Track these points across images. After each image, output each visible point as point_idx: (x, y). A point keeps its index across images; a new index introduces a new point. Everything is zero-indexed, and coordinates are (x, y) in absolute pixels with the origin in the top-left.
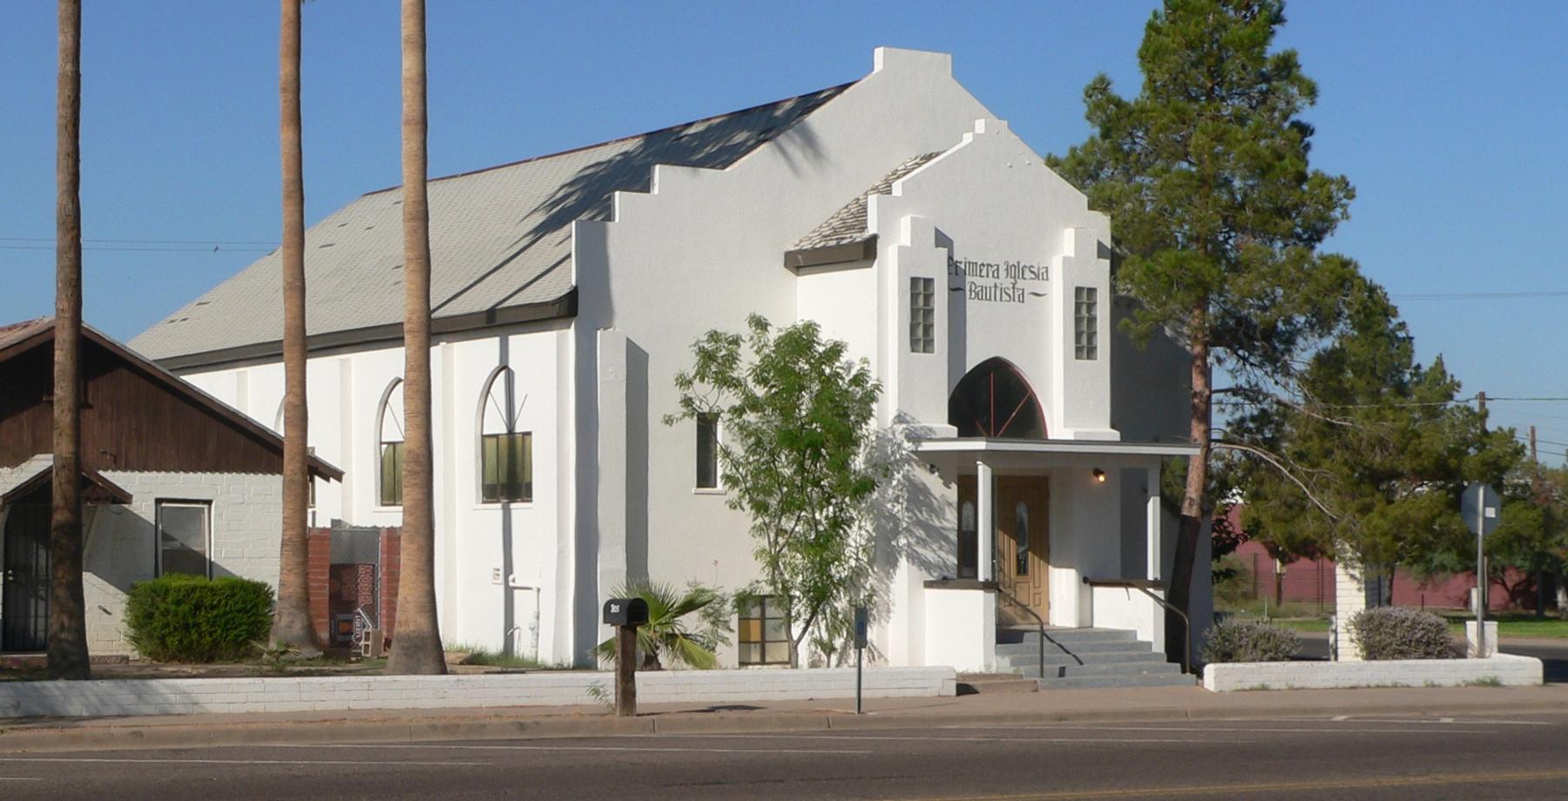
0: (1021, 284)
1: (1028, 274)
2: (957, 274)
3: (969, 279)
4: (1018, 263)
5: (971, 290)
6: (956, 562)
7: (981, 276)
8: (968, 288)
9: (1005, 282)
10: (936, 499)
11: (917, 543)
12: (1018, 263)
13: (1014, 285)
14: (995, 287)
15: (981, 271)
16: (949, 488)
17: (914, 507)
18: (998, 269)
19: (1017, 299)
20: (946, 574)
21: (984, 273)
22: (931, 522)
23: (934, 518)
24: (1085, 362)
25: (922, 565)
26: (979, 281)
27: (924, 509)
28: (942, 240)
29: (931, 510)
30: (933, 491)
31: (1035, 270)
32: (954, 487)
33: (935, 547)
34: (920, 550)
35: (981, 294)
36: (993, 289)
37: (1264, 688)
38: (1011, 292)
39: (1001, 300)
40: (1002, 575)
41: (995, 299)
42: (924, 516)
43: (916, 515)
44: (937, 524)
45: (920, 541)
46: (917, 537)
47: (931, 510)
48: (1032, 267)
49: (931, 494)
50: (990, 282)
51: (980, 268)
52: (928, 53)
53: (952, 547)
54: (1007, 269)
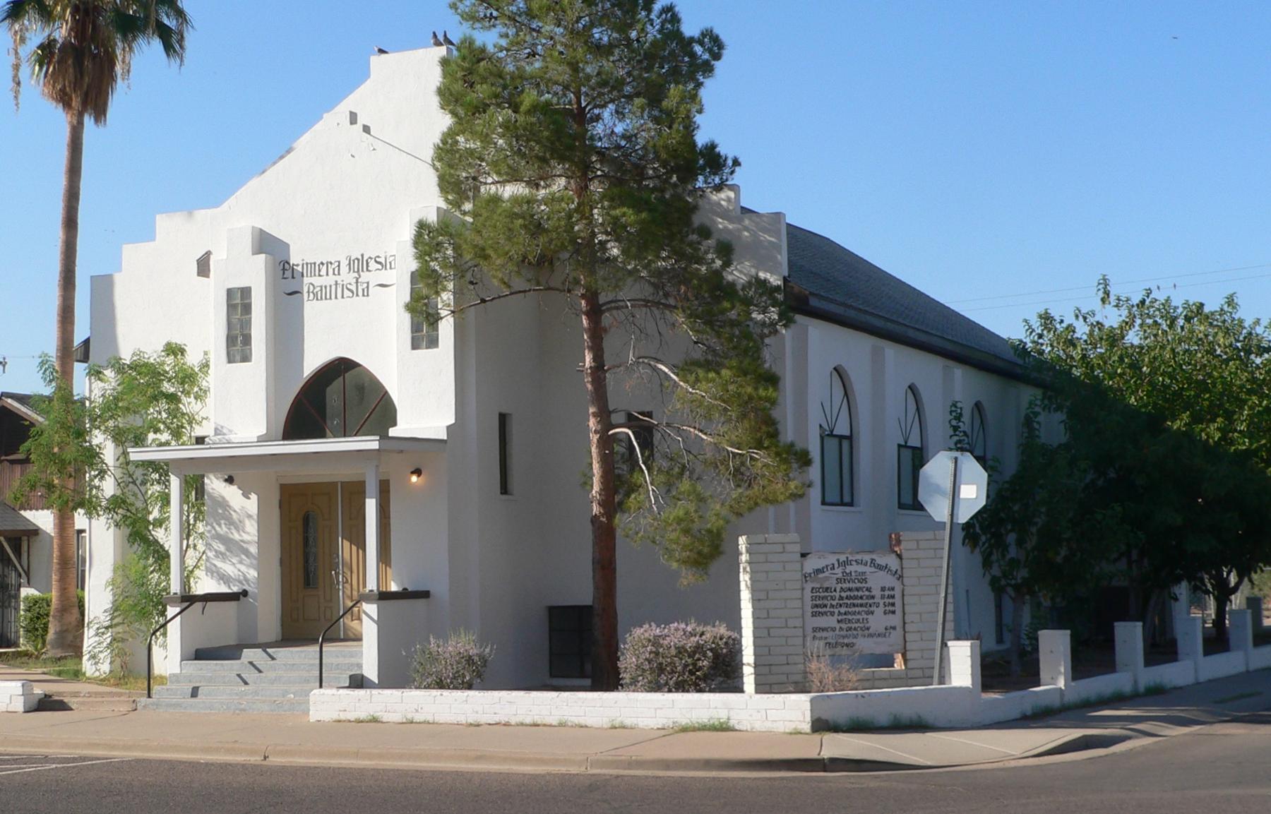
0: (365, 276)
1: (373, 265)
2: (293, 277)
3: (306, 280)
4: (362, 255)
5: (308, 292)
6: (256, 575)
7: (320, 275)
8: (305, 289)
9: (347, 277)
10: (235, 511)
11: (217, 557)
12: (362, 255)
13: (357, 279)
14: (336, 283)
15: (320, 271)
16: (249, 498)
17: (212, 520)
18: (339, 266)
20: (246, 587)
22: (231, 536)
23: (234, 531)
24: (423, 353)
25: (222, 579)
26: (317, 281)
27: (222, 522)
28: (265, 243)
29: (231, 523)
30: (232, 503)
31: (382, 260)
32: (254, 497)
33: (234, 561)
34: (219, 564)
35: (322, 294)
36: (333, 287)
37: (375, 720)
38: (353, 288)
39: (343, 297)
40: (348, 586)
41: (336, 298)
42: (223, 530)
43: (215, 529)
44: (236, 536)
45: (218, 554)
46: (216, 551)
47: (231, 523)
48: (378, 257)
49: (229, 507)
50: (329, 280)
51: (315, 268)
52: (421, 51)
53: (255, 562)
54: (349, 264)
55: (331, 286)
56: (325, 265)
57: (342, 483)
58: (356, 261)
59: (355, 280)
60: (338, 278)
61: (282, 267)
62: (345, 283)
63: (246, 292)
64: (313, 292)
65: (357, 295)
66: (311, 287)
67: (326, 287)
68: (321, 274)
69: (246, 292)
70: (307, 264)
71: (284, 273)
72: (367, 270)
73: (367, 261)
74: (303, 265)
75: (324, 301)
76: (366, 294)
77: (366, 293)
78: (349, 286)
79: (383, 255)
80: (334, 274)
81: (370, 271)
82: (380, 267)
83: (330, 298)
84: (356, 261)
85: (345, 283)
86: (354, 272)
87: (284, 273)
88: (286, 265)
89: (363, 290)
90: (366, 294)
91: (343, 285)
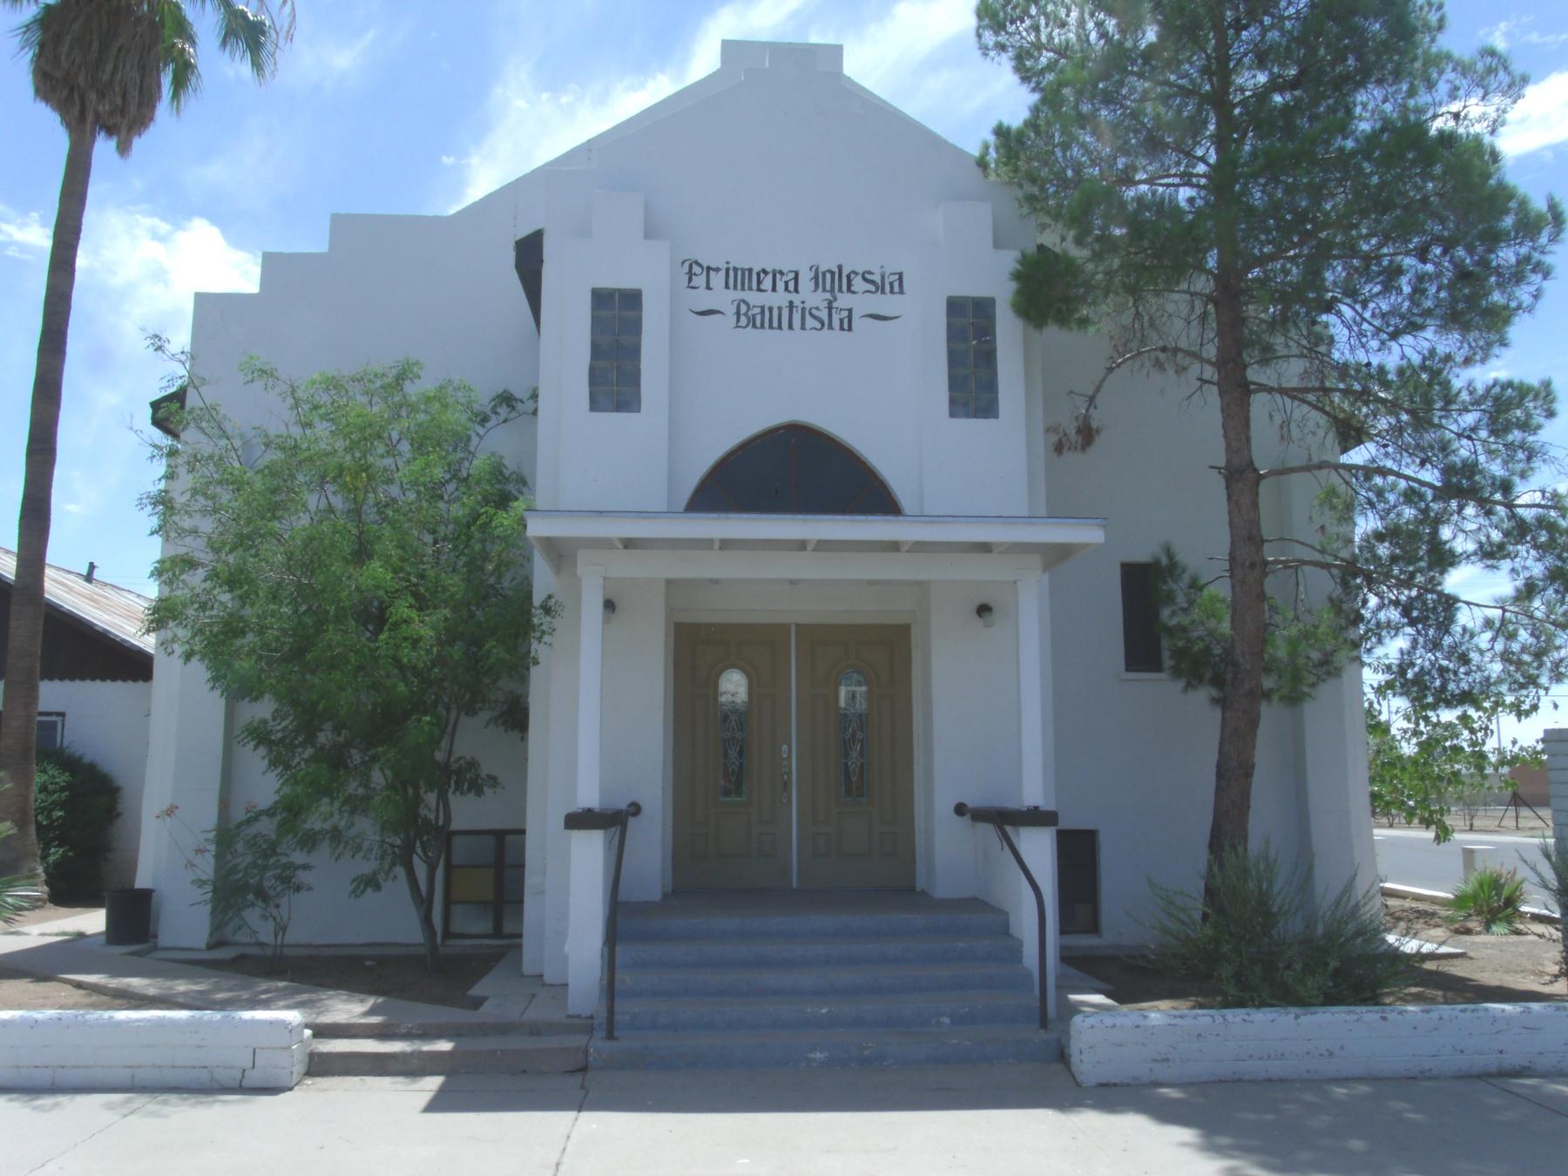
0: (844, 300)
1: (858, 284)
2: (708, 287)
4: (840, 268)
7: (759, 290)
9: (817, 300)
12: (840, 268)
13: (830, 303)
15: (759, 282)
18: (796, 279)
19: (836, 323)
21: (767, 283)
31: (877, 278)
38: (824, 315)
39: (803, 328)
41: (791, 327)
48: (870, 273)
50: (780, 299)
54: (816, 278)
55: (780, 309)
56: (771, 275)
57: (797, 625)
58: (828, 276)
59: (825, 304)
60: (796, 299)
61: (687, 270)
62: (808, 306)
63: (632, 299)
64: (746, 314)
65: (831, 327)
66: (743, 308)
67: (771, 309)
68: (762, 287)
69: (632, 299)
70: (735, 270)
71: (690, 280)
72: (849, 289)
73: (848, 276)
74: (727, 270)
75: (767, 331)
76: (846, 326)
77: (847, 325)
78: (814, 311)
79: (877, 271)
80: (786, 289)
81: (854, 292)
82: (872, 288)
83: (780, 327)
84: (828, 276)
85: (808, 306)
86: (824, 290)
87: (690, 280)
88: (696, 269)
89: (841, 321)
90: (846, 326)
91: (803, 309)
